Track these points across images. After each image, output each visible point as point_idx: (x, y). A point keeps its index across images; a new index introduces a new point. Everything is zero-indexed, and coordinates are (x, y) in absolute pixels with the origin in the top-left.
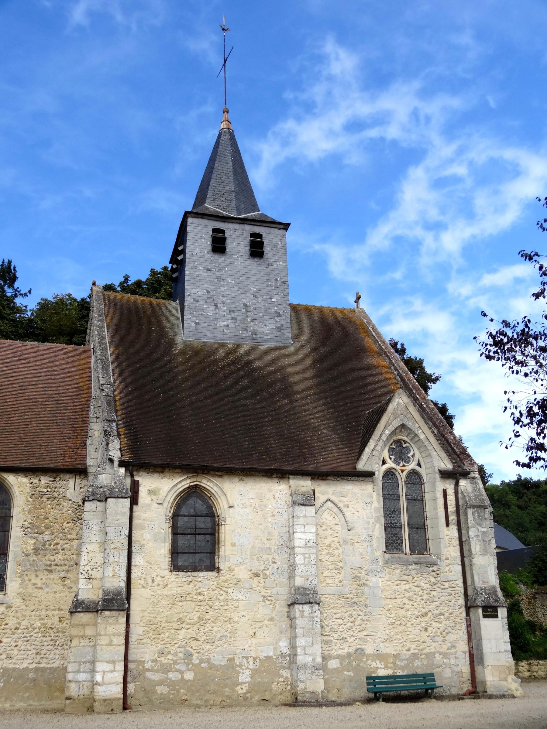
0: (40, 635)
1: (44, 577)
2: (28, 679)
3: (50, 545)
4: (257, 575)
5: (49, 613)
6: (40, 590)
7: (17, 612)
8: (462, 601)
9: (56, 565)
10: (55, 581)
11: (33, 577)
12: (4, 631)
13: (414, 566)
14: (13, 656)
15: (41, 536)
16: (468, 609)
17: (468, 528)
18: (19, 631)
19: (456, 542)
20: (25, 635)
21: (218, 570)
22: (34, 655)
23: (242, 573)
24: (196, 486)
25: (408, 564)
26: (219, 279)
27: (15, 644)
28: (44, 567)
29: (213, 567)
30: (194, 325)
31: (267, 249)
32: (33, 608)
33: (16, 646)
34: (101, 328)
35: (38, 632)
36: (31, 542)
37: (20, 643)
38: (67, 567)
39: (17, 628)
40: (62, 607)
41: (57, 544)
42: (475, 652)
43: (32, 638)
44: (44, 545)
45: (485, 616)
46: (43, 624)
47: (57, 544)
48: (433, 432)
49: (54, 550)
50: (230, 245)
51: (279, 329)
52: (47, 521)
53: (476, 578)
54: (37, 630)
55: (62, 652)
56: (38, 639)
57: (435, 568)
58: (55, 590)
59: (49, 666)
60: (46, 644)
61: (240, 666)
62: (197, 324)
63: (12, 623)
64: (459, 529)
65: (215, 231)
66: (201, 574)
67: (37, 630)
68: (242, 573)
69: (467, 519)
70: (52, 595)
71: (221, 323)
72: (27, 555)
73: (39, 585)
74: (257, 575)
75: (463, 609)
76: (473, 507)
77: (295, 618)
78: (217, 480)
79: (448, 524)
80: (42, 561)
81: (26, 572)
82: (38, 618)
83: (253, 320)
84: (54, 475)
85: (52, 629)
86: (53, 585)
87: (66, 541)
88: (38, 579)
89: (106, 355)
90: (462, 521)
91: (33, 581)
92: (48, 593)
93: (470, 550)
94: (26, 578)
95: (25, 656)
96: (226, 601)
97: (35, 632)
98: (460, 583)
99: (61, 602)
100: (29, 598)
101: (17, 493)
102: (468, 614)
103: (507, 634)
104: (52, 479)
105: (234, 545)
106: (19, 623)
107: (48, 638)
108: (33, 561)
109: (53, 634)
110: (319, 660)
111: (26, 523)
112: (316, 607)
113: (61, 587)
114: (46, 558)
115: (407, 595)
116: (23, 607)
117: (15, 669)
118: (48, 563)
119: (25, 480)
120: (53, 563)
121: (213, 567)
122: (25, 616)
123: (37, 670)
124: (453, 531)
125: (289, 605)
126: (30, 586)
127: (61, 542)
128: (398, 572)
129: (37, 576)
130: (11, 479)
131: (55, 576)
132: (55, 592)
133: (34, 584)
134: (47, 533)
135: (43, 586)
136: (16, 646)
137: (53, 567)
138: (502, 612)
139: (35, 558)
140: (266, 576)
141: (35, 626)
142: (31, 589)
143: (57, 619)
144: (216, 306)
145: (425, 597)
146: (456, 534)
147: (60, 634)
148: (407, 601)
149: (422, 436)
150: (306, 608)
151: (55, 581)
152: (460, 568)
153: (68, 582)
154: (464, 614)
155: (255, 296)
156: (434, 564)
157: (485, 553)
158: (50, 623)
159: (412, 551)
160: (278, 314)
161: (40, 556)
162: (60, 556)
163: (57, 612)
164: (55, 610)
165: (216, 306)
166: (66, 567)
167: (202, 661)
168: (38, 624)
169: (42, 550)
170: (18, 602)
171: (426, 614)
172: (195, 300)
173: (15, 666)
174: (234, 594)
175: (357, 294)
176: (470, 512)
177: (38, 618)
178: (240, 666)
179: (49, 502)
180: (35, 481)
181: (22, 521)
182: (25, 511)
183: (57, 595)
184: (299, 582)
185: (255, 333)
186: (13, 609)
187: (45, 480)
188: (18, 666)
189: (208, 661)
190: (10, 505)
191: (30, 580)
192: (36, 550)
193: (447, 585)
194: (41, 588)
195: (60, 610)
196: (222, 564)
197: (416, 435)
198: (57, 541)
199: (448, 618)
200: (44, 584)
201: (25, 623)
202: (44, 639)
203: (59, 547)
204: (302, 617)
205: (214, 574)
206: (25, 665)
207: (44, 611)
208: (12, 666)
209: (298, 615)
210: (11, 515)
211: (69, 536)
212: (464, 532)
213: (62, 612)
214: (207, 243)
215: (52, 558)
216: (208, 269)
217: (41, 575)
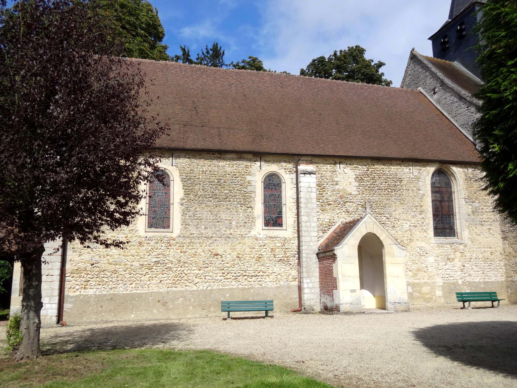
0: (483, 263)
1: (480, 229)
2: (481, 288)
3: (479, 209)
5: (485, 249)
6: (479, 236)
7: (470, 249)
9: (484, 221)
10: (485, 231)
11: (474, 228)
12: (465, 260)
14: (471, 274)
15: (474, 204)
18: (472, 260)
20: (475, 262)
22: (481, 274)
27: (471, 268)
28: (479, 223)
32: (477, 246)
33: (472, 269)
35: (481, 261)
36: (470, 207)
37: (473, 267)
38: (489, 223)
39: (471, 259)
40: (491, 246)
41: (483, 209)
43: (479, 264)
44: (476, 210)
46: (483, 256)
47: (483, 209)
49: (482, 212)
52: (475, 195)
54: (481, 260)
55: (494, 272)
56: (482, 265)
58: (486, 236)
59: (489, 280)
60: (486, 268)
63: (468, 255)
67: (481, 260)
70: (485, 239)
72: (469, 216)
73: (478, 233)
80: (477, 219)
81: (471, 226)
82: (480, 253)
84: (475, 167)
85: (487, 259)
86: (485, 233)
87: (486, 207)
88: (477, 229)
91: (475, 231)
92: (483, 238)
94: (471, 229)
95: (477, 275)
97: (480, 260)
99: (491, 243)
100: (474, 241)
101: (459, 178)
104: (474, 169)
106: (471, 256)
107: (487, 265)
108: (473, 219)
109: (489, 262)
111: (466, 196)
113: (489, 234)
114: (479, 217)
116: (472, 246)
117: (474, 282)
118: (480, 220)
119: (461, 170)
120: (483, 220)
122: (473, 251)
123: (484, 282)
126: (474, 234)
127: (484, 208)
129: (476, 228)
130: (455, 169)
131: (485, 228)
132: (486, 237)
133: (476, 233)
134: (477, 202)
135: (481, 234)
136: (472, 269)
137: (483, 223)
139: (473, 217)
141: (479, 257)
142: (474, 235)
143: (490, 253)
147: (492, 262)
151: (485, 231)
153: (491, 231)
158: (486, 256)
161: (475, 216)
162: (484, 216)
163: (489, 249)
164: (487, 248)
166: (489, 223)
168: (481, 256)
169: (476, 212)
170: (469, 243)
173: (473, 280)
177: (480, 253)
179: (475, 183)
180: (466, 170)
181: (464, 194)
182: (464, 189)
183: (488, 239)
186: (468, 247)
187: (470, 170)
188: (474, 280)
190: (451, 185)
191: (473, 230)
192: (473, 212)
194: (479, 235)
195: (490, 248)
198: (483, 207)
200: (480, 232)
201: (474, 255)
202: (485, 265)
203: (483, 210)
206: (477, 280)
207: (482, 248)
208: (472, 280)
210: (453, 191)
211: (487, 204)
213: (491, 249)
215: (481, 217)
217: (478, 228)
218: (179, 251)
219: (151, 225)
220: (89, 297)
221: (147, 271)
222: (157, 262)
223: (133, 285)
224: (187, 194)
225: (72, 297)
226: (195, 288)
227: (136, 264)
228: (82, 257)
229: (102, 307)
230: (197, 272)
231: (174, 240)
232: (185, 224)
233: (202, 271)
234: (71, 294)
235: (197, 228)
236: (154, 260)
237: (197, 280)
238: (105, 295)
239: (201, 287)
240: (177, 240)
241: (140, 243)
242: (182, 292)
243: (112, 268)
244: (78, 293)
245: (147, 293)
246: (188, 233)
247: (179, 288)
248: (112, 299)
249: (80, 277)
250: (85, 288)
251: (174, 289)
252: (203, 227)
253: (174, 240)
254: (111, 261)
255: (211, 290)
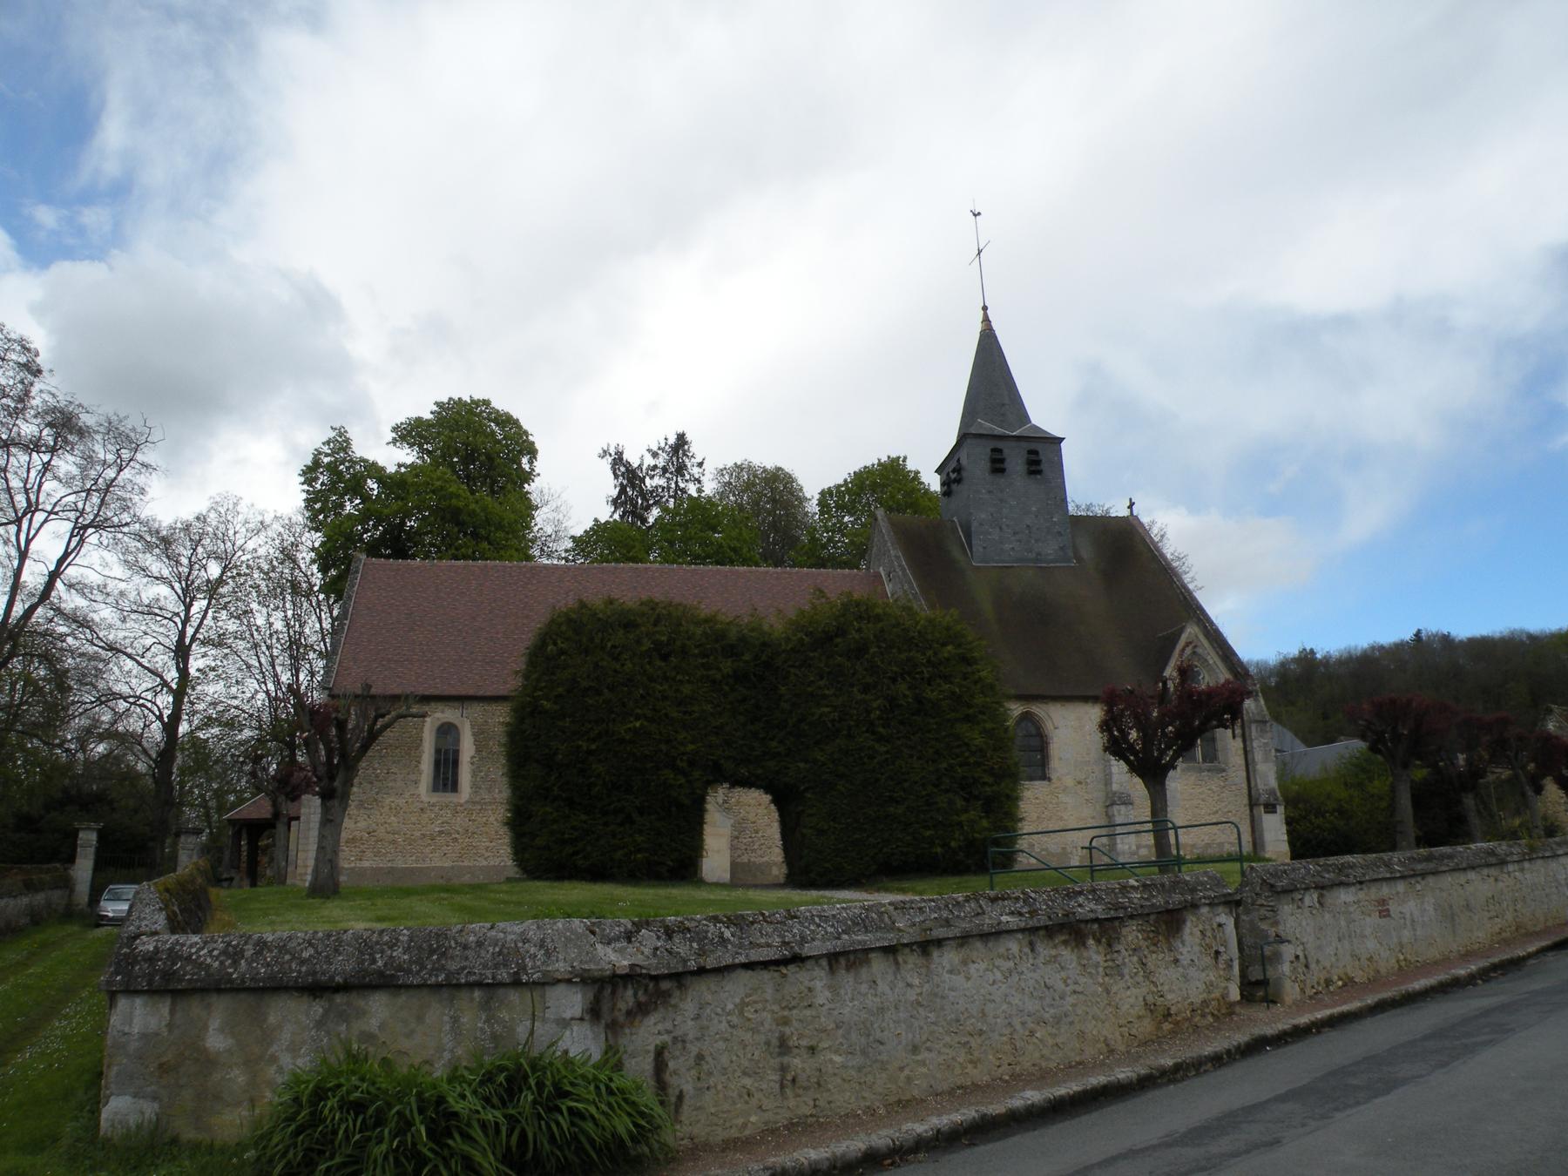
4: (1080, 783)
8: (1246, 801)
13: (1206, 773)
16: (1252, 804)
17: (1252, 740)
19: (1241, 752)
21: (1049, 780)
23: (1069, 782)
24: (1027, 712)
25: (1201, 770)
26: (1001, 501)
29: (1044, 777)
30: (981, 550)
31: (1044, 466)
34: (897, 557)
42: (1258, 841)
45: (1265, 812)
48: (1217, 653)
50: (1009, 465)
51: (1062, 548)
53: (1258, 781)
57: (1224, 774)
61: (1071, 853)
62: (984, 548)
64: (1244, 741)
65: (994, 450)
66: (1037, 783)
68: (1069, 782)
69: (1251, 733)
71: (1007, 546)
74: (1080, 783)
75: (1248, 808)
76: (1257, 721)
77: (1113, 815)
78: (1044, 706)
79: (1234, 737)
83: (1037, 541)
89: (913, 589)
90: (1247, 734)
93: (1254, 759)
96: (1057, 804)
98: (1245, 785)
102: (1251, 810)
103: (1284, 828)
105: (1060, 759)
110: (1134, 847)
112: (1131, 807)
115: (1201, 797)
121: (1044, 777)
124: (1239, 741)
125: (1107, 806)
128: (1193, 778)
138: (1280, 809)
140: (1087, 783)
144: (1001, 528)
145: (1216, 798)
146: (1241, 745)
148: (1200, 801)
149: (1211, 662)
150: (1123, 808)
152: (1244, 774)
154: (1248, 811)
155: (1036, 516)
156: (1224, 770)
157: (1266, 760)
159: (1204, 761)
160: (1059, 533)
165: (1001, 528)
167: (1043, 850)
171: (1217, 812)
172: (981, 524)
174: (1063, 798)
175: (1131, 500)
176: (1253, 727)
178: (1071, 853)
184: (1115, 787)
185: (1039, 554)
189: (1046, 850)
193: (1233, 787)
196: (1054, 776)
197: (1206, 660)
199: (1235, 815)
204: (1120, 814)
205: (1046, 782)
209: (1116, 813)
212: (1248, 743)
214: (985, 464)
216: (990, 492)
218: (467, 820)
219: (435, 788)
220: (365, 869)
221: (430, 842)
222: (441, 832)
223: (414, 858)
224: (478, 751)
225: (347, 869)
226: (485, 863)
227: (418, 834)
228: (359, 825)
229: (378, 881)
230: (488, 844)
231: (461, 806)
232: (475, 787)
233: (493, 844)
234: (346, 866)
235: (489, 792)
236: (437, 829)
237: (487, 854)
238: (382, 868)
239: (492, 863)
240: (466, 806)
241: (422, 809)
242: (470, 867)
243: (391, 837)
244: (353, 865)
245: (428, 868)
246: (478, 799)
247: (466, 863)
248: (389, 872)
249: (355, 847)
250: (361, 860)
251: (461, 863)
252: (497, 791)
253: (461, 806)
254: (389, 830)
255: (505, 866)
